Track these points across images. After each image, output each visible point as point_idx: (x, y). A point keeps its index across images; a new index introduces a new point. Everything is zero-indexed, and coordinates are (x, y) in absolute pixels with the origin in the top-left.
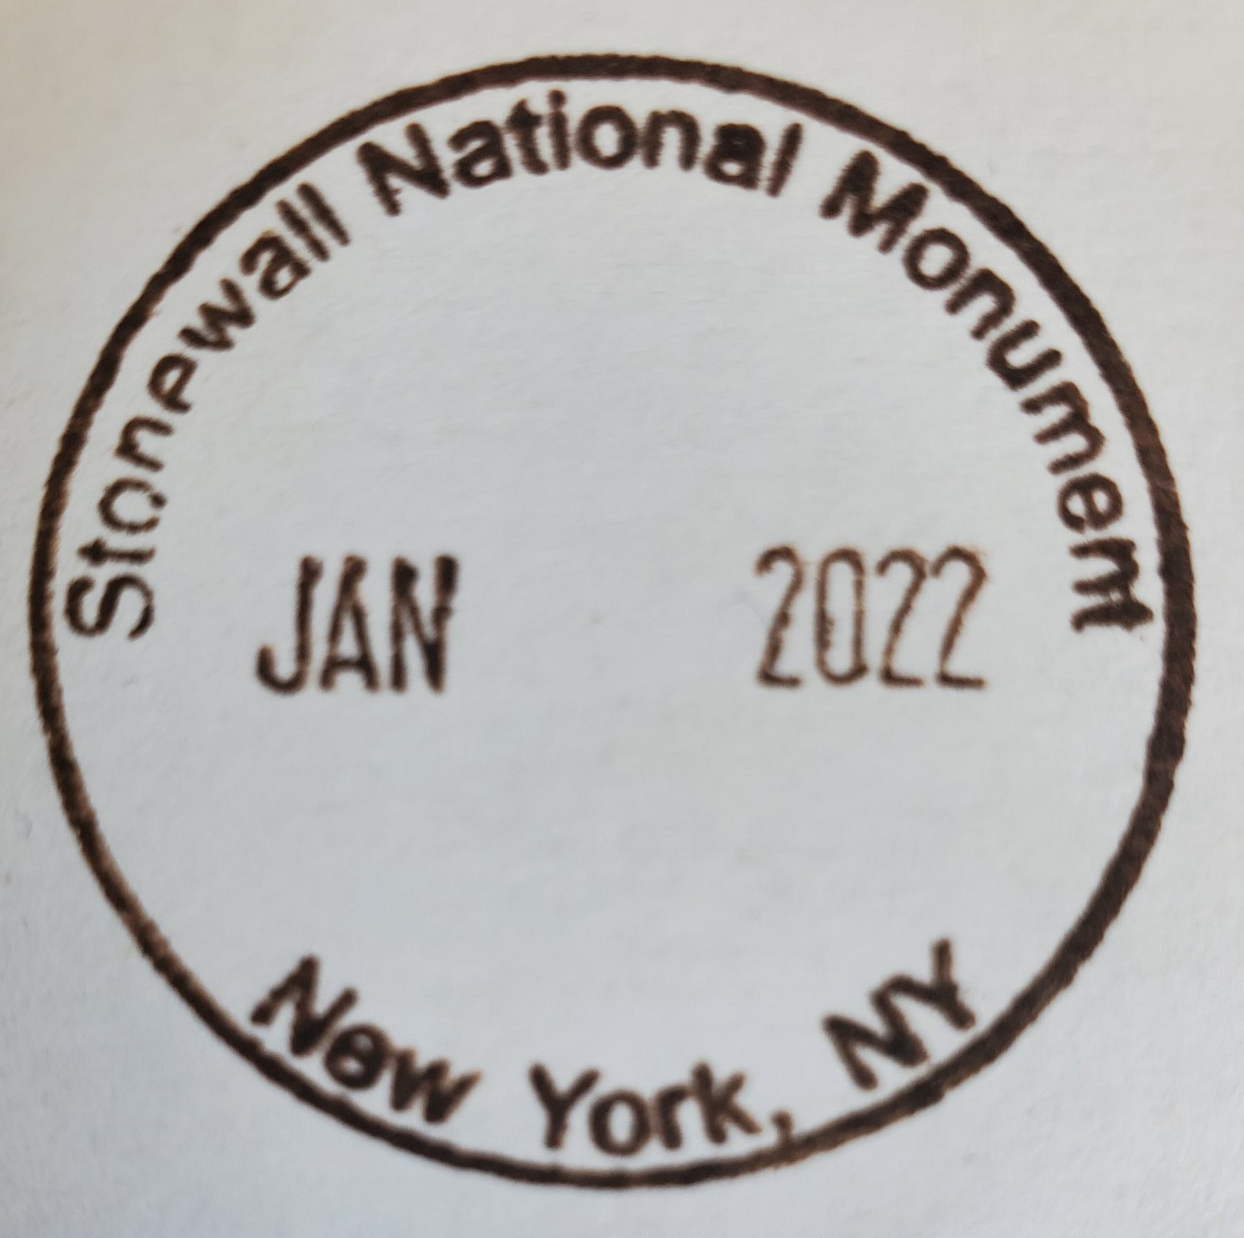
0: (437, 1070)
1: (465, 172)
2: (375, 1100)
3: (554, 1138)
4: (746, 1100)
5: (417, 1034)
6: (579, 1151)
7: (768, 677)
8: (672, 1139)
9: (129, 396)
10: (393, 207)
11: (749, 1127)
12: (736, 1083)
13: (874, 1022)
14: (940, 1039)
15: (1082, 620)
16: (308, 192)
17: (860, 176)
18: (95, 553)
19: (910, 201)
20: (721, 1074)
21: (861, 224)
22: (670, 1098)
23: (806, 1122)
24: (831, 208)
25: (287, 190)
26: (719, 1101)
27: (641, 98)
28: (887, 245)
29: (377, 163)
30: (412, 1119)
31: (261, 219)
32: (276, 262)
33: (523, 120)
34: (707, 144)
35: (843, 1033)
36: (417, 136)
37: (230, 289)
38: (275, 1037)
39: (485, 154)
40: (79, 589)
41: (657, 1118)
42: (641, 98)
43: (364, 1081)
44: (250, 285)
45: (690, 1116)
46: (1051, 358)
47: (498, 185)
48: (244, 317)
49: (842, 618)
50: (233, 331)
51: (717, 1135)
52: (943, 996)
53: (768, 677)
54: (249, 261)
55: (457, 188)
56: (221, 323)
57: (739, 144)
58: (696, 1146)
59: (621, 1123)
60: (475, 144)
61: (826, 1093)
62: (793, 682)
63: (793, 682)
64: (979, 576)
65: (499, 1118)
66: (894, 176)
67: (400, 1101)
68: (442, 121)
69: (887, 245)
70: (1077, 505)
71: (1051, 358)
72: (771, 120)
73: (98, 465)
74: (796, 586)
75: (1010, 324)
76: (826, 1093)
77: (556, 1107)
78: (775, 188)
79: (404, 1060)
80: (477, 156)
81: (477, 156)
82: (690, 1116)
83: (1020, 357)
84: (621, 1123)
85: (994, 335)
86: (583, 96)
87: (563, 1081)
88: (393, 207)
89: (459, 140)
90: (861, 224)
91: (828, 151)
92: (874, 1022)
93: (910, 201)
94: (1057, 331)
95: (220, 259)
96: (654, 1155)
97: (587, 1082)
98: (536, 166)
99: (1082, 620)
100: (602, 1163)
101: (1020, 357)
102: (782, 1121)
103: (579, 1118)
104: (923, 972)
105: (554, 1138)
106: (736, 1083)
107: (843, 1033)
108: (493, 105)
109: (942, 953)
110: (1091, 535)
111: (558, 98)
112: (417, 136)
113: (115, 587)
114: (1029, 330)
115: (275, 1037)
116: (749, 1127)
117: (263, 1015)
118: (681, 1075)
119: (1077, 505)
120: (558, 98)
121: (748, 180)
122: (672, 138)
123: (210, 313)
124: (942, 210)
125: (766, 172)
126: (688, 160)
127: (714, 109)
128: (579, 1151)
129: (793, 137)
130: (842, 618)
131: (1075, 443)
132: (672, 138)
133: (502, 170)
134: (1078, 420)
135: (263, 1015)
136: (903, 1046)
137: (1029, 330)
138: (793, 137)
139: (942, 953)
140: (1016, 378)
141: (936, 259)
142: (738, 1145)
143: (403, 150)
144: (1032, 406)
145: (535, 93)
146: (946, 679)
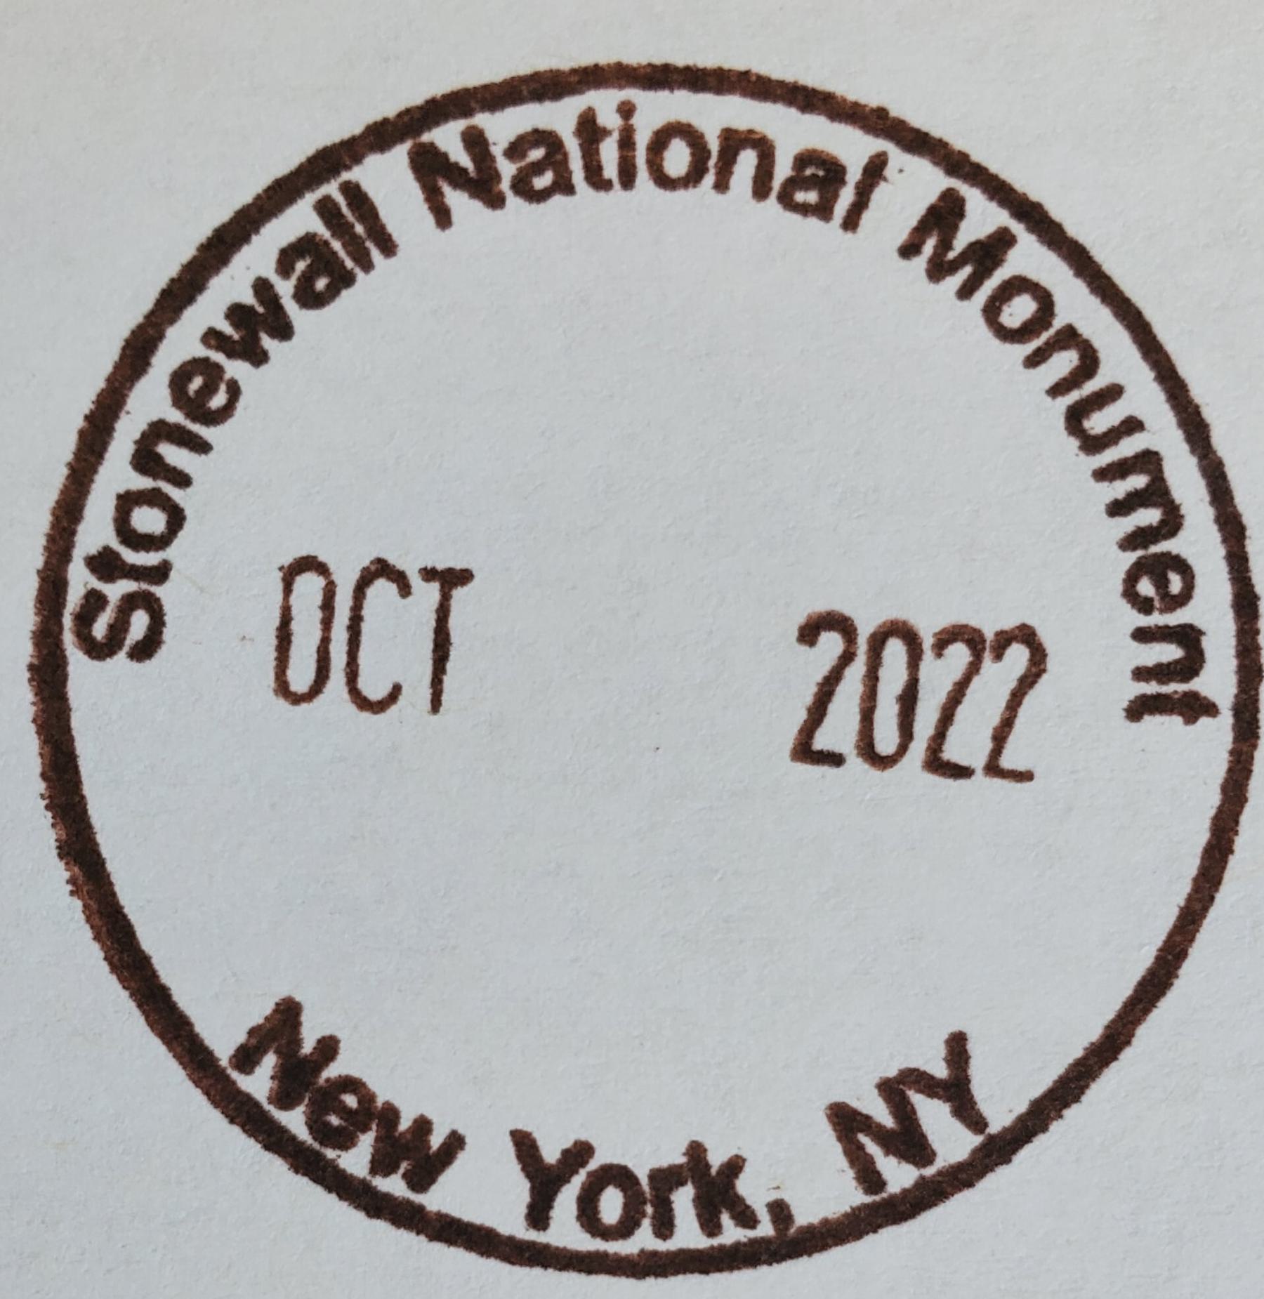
0: (423, 1126)
1: (522, 187)
2: (356, 1160)
3: (538, 1215)
4: (745, 1186)
5: (408, 1092)
6: (565, 1229)
7: (805, 751)
8: (664, 1226)
9: (150, 400)
10: (443, 217)
11: (746, 1218)
12: (734, 1167)
13: (882, 1115)
14: (951, 1141)
15: (1138, 709)
16: (354, 194)
17: (945, 214)
18: (105, 565)
19: (992, 250)
20: (716, 1159)
21: (938, 270)
22: (666, 1179)
23: (805, 1215)
24: (909, 250)
25: (331, 189)
26: (717, 1189)
27: (714, 114)
28: (966, 292)
29: (430, 167)
30: (394, 1185)
31: (301, 219)
32: (323, 271)
33: (589, 129)
34: (783, 169)
35: (846, 1121)
36: (475, 141)
37: (262, 288)
38: (258, 1083)
39: (545, 170)
40: (94, 601)
41: (650, 1197)
42: (714, 114)
43: (345, 1140)
44: (285, 289)
45: (683, 1200)
46: (1132, 425)
47: (558, 200)
48: (284, 331)
49: (891, 692)
50: (267, 342)
51: (710, 1226)
52: (957, 1092)
53: (805, 751)
54: (285, 263)
55: (512, 201)
56: (256, 327)
57: (820, 173)
58: (689, 1233)
59: (611, 1205)
60: (537, 154)
61: (827, 1190)
62: (835, 759)
63: (835, 759)
64: (1038, 657)
65: (484, 1188)
66: (982, 217)
67: (381, 1165)
68: (501, 127)
69: (966, 292)
70: (1146, 587)
71: (1132, 425)
72: (852, 148)
73: (117, 473)
74: (847, 658)
75: (1091, 387)
76: (827, 1190)
77: (544, 1182)
78: (851, 222)
79: (390, 1115)
80: (538, 168)
81: (538, 168)
82: (683, 1200)
83: (1098, 423)
84: (611, 1205)
85: (1074, 396)
86: (654, 109)
87: (551, 1154)
88: (443, 217)
89: (516, 150)
90: (938, 270)
91: (914, 185)
92: (882, 1115)
93: (992, 250)
94: (1143, 396)
95: (257, 257)
96: (644, 1239)
97: (579, 1153)
98: (596, 179)
99: (1138, 709)
100: (584, 1242)
101: (1098, 423)
102: (780, 1211)
103: (566, 1201)
104: (940, 1071)
105: (538, 1215)
106: (734, 1167)
107: (846, 1121)
108: (560, 116)
109: (957, 1047)
110: (1157, 619)
111: (626, 110)
112: (475, 141)
113: (130, 603)
114: (1113, 393)
115: (258, 1083)
116: (746, 1218)
117: (246, 1059)
118: (677, 1157)
119: (1146, 587)
120: (626, 110)
121: (823, 210)
122: (747, 161)
123: (237, 313)
124: (1029, 257)
125: (846, 197)
126: (761, 188)
127: (794, 133)
128: (565, 1229)
129: (875, 170)
130: (891, 692)
131: (1149, 516)
132: (747, 161)
133: (564, 186)
134: (1157, 493)
135: (246, 1059)
136: (909, 1142)
137: (1113, 393)
138: (875, 170)
139: (957, 1047)
140: (1092, 444)
141: (1020, 310)
142: (732, 1233)
143: (460, 157)
144: (1102, 475)
145: (604, 103)
146: (993, 768)
